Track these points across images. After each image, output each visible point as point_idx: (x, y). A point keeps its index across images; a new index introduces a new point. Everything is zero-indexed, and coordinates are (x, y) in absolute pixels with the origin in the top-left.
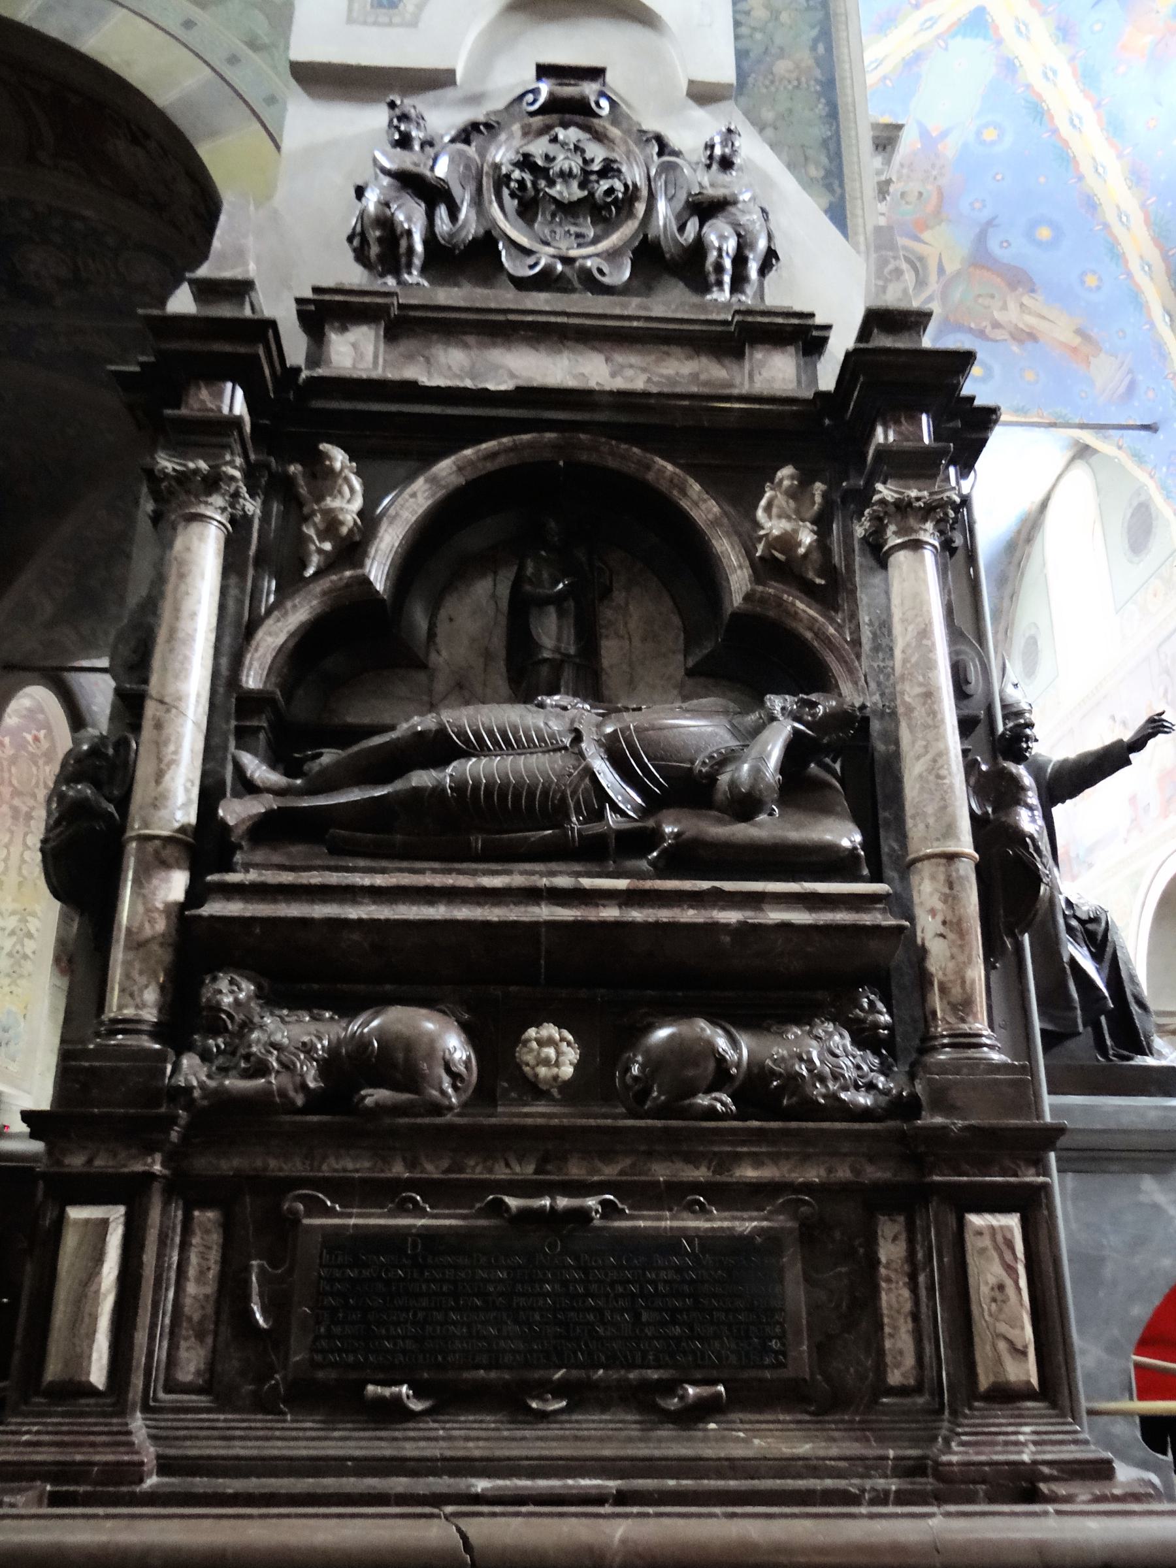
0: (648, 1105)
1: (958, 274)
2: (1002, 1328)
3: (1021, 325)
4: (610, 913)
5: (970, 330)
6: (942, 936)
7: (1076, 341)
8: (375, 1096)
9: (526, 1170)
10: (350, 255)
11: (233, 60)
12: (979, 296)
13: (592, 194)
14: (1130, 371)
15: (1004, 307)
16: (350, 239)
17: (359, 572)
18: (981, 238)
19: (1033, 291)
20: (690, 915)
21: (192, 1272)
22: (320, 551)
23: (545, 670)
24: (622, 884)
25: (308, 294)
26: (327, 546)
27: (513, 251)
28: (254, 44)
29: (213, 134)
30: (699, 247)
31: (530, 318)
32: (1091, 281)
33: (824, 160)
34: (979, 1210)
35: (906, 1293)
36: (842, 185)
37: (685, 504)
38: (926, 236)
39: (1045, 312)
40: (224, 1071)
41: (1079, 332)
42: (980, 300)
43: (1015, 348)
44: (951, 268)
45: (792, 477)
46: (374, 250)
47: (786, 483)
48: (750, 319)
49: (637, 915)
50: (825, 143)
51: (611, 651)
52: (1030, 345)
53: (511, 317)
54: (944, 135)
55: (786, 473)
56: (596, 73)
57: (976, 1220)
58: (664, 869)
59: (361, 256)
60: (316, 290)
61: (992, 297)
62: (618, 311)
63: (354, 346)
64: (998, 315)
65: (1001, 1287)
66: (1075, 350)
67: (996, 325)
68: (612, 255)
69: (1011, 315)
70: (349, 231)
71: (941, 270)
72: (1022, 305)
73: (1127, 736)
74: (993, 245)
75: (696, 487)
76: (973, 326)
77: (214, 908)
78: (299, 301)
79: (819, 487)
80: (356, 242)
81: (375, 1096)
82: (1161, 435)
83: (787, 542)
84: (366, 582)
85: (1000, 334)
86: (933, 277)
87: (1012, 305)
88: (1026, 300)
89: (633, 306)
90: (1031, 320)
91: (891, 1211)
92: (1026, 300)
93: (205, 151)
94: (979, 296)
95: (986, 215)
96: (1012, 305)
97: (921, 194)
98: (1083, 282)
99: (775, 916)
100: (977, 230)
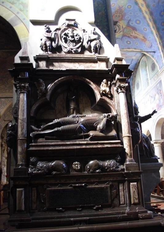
0: (90, 172)
1: (125, 28)
2: (135, 196)
4: (84, 147)
5: (127, 36)
6: (127, 147)
7: (143, 38)
8: (54, 173)
9: (75, 181)
10: (41, 49)
11: (18, 13)
13: (75, 39)
14: (151, 43)
15: (132, 33)
16: (40, 47)
17: (45, 98)
18: (128, 22)
19: (136, 31)
20: (95, 146)
21: (33, 196)
22: (40, 95)
23: (72, 110)
24: (85, 142)
25: (35, 56)
26: (41, 94)
27: (64, 48)
28: (21, 10)
29: (16, 25)
30: (90, 47)
31: (67, 58)
32: (145, 29)
33: (107, 28)
34: (132, 182)
35: (123, 193)
36: (109, 32)
37: (90, 85)
39: (138, 34)
40: (35, 170)
41: (143, 37)
43: (134, 39)
45: (106, 81)
46: (44, 49)
47: (105, 82)
48: (98, 58)
49: (88, 147)
50: (107, 25)
51: (81, 106)
52: (136, 39)
53: (64, 58)
54: (122, 7)
55: (105, 81)
56: (74, 20)
57: (131, 184)
58: (91, 140)
59: (42, 49)
60: (37, 56)
61: (130, 31)
62: (79, 57)
63: (42, 63)
64: (131, 34)
65: (134, 191)
66: (143, 40)
67: (131, 36)
68: (78, 48)
69: (134, 34)
70: (40, 46)
71: (123, 27)
72: (135, 33)
73: (151, 113)
74: (130, 23)
75: (92, 83)
77: (31, 149)
78: (34, 57)
79: (109, 82)
80: (41, 47)
81: (54, 173)
82: (156, 53)
83: (105, 91)
84: (47, 99)
86: (121, 28)
87: (134, 33)
88: (135, 32)
89: (81, 56)
90: (136, 35)
91: (121, 183)
92: (135, 32)
93: (15, 28)
95: (129, 19)
96: (134, 33)
97: (119, 16)
98: (144, 30)
99: (106, 146)
100: (128, 21)
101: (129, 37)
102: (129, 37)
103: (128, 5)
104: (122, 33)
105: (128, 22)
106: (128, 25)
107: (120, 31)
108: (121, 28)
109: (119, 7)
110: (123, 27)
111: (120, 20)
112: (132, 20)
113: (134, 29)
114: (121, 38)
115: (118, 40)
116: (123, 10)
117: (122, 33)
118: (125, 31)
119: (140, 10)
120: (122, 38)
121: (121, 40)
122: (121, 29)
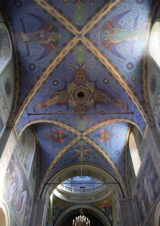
1: (68, 100)
3: (54, 98)
7: (45, 104)
12: (63, 97)
15: (58, 98)
18: (68, 107)
19: (56, 104)
38: (76, 104)
39: (52, 103)
42: (63, 97)
44: (70, 100)
54: (80, 119)
66: (44, 103)
67: (58, 94)
69: (56, 98)
71: (71, 99)
72: (56, 101)
76: (61, 92)
85: (56, 93)
86: (72, 97)
87: (57, 100)
88: (56, 102)
90: (53, 100)
92: (56, 102)
94: (63, 97)
95: (69, 110)
96: (57, 100)
100: (69, 107)
101: (59, 92)
102: (59, 91)
103: (76, 122)
104: (69, 91)
105: (68, 107)
106: (66, 104)
107: (72, 93)
108: (72, 97)
109: (83, 119)
110: (71, 99)
111: (77, 106)
112: (66, 111)
113: (59, 104)
114: (67, 83)
115: (69, 80)
116: (78, 117)
117: (69, 91)
118: (66, 96)
119: (63, 122)
120: (66, 85)
121: (65, 81)
122: (71, 96)
